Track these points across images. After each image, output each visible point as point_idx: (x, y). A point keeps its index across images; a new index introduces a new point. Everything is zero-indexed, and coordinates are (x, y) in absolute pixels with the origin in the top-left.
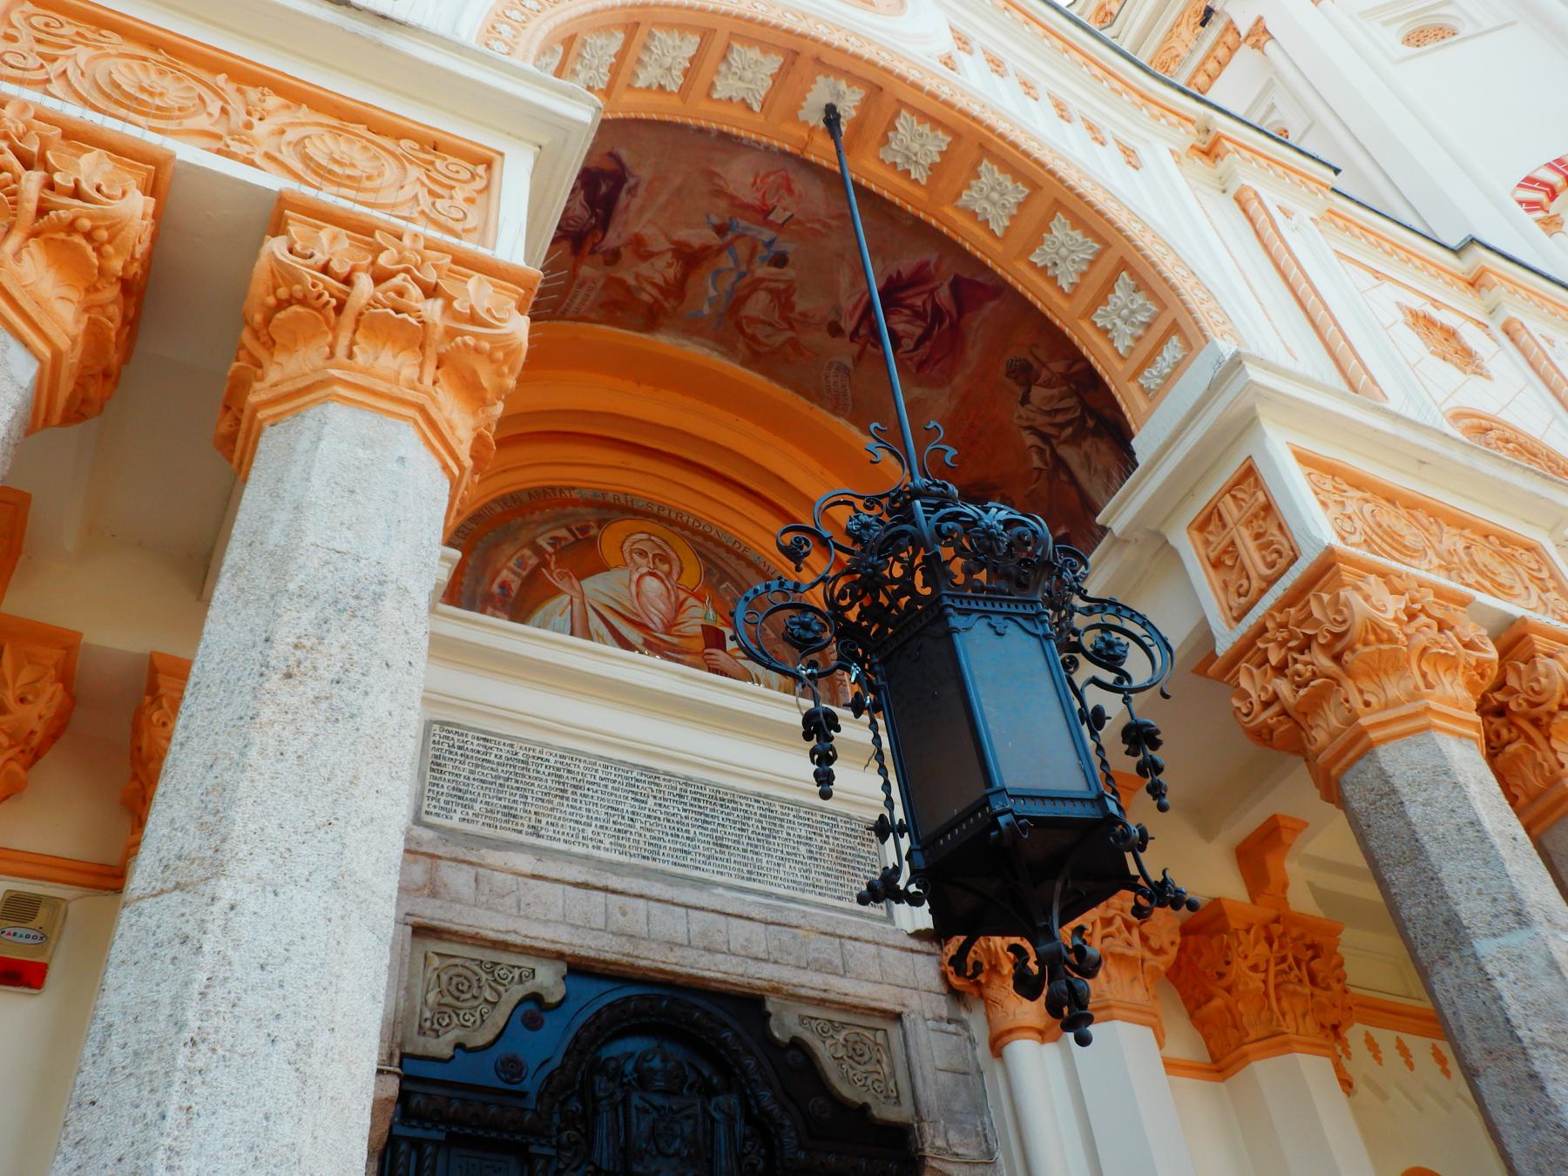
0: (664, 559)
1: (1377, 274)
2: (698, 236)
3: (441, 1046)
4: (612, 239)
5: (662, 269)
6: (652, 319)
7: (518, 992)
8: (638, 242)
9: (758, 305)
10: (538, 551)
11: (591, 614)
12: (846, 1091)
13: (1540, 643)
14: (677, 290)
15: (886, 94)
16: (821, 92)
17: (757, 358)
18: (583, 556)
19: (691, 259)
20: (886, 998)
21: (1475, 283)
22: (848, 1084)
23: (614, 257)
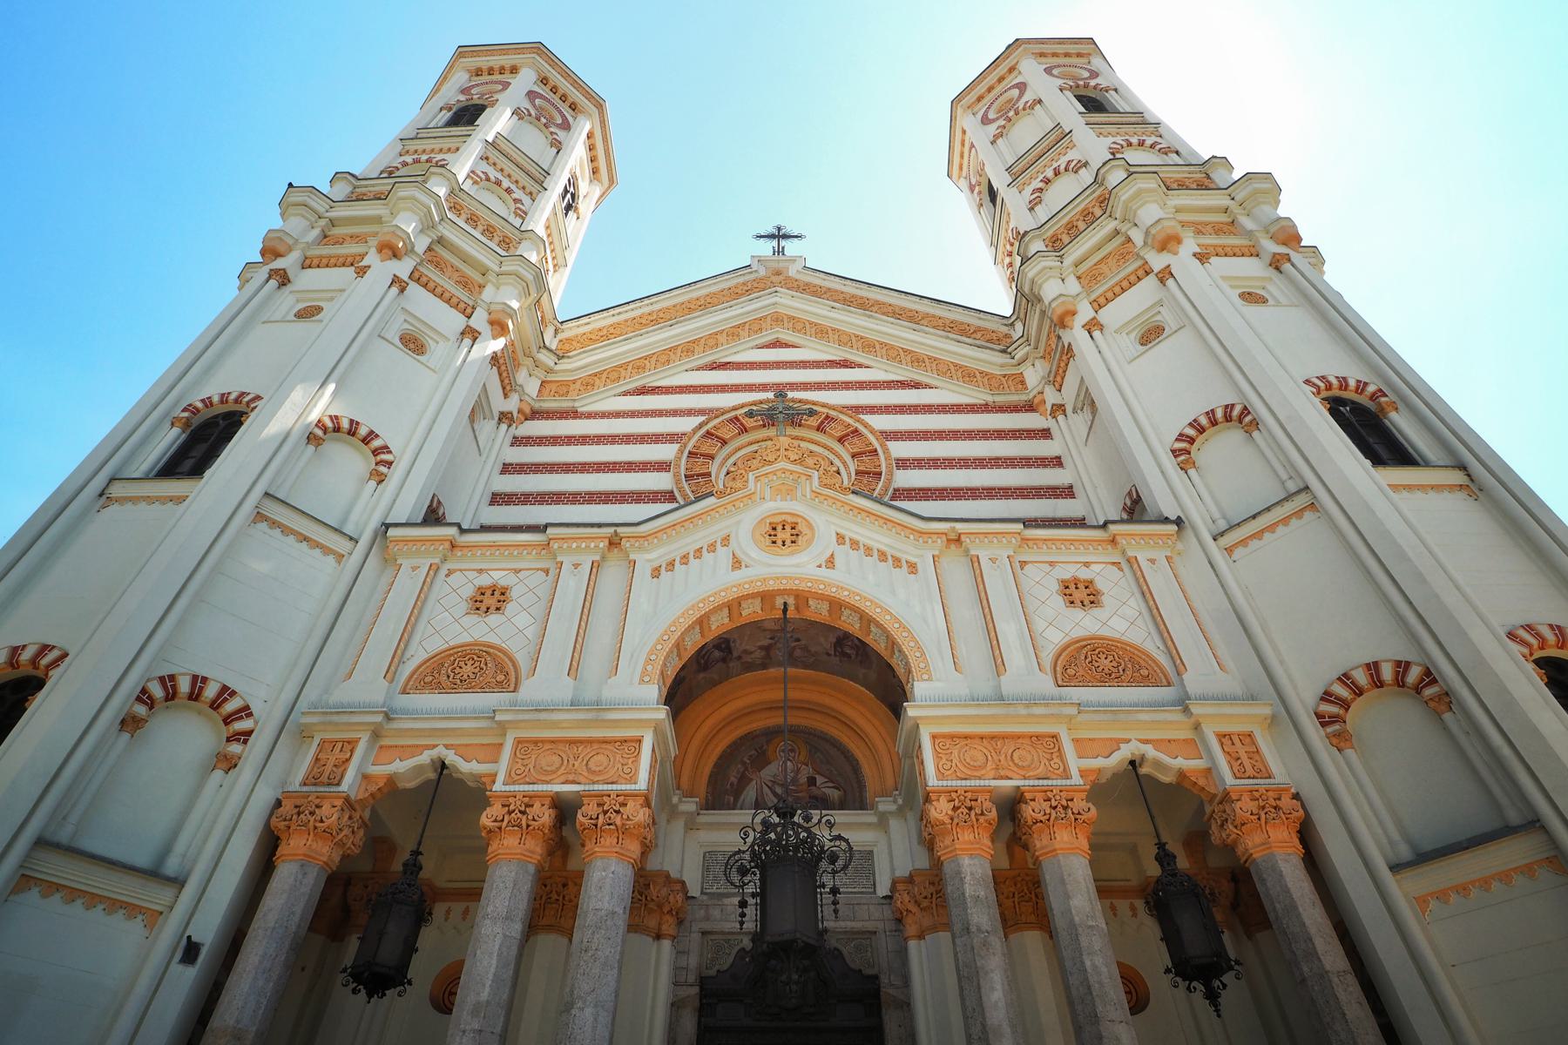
0: (792, 750)
1: (1052, 564)
2: (766, 642)
3: (713, 972)
4: (735, 654)
5: (759, 654)
6: (764, 666)
7: (737, 949)
8: (745, 652)
9: (798, 653)
10: (744, 763)
11: (766, 789)
12: (852, 966)
13: (1028, 796)
14: (768, 656)
15: (802, 598)
16: (779, 602)
17: (806, 667)
18: (761, 761)
19: (767, 649)
20: (869, 926)
21: (1113, 541)
22: (855, 962)
23: (739, 658)
